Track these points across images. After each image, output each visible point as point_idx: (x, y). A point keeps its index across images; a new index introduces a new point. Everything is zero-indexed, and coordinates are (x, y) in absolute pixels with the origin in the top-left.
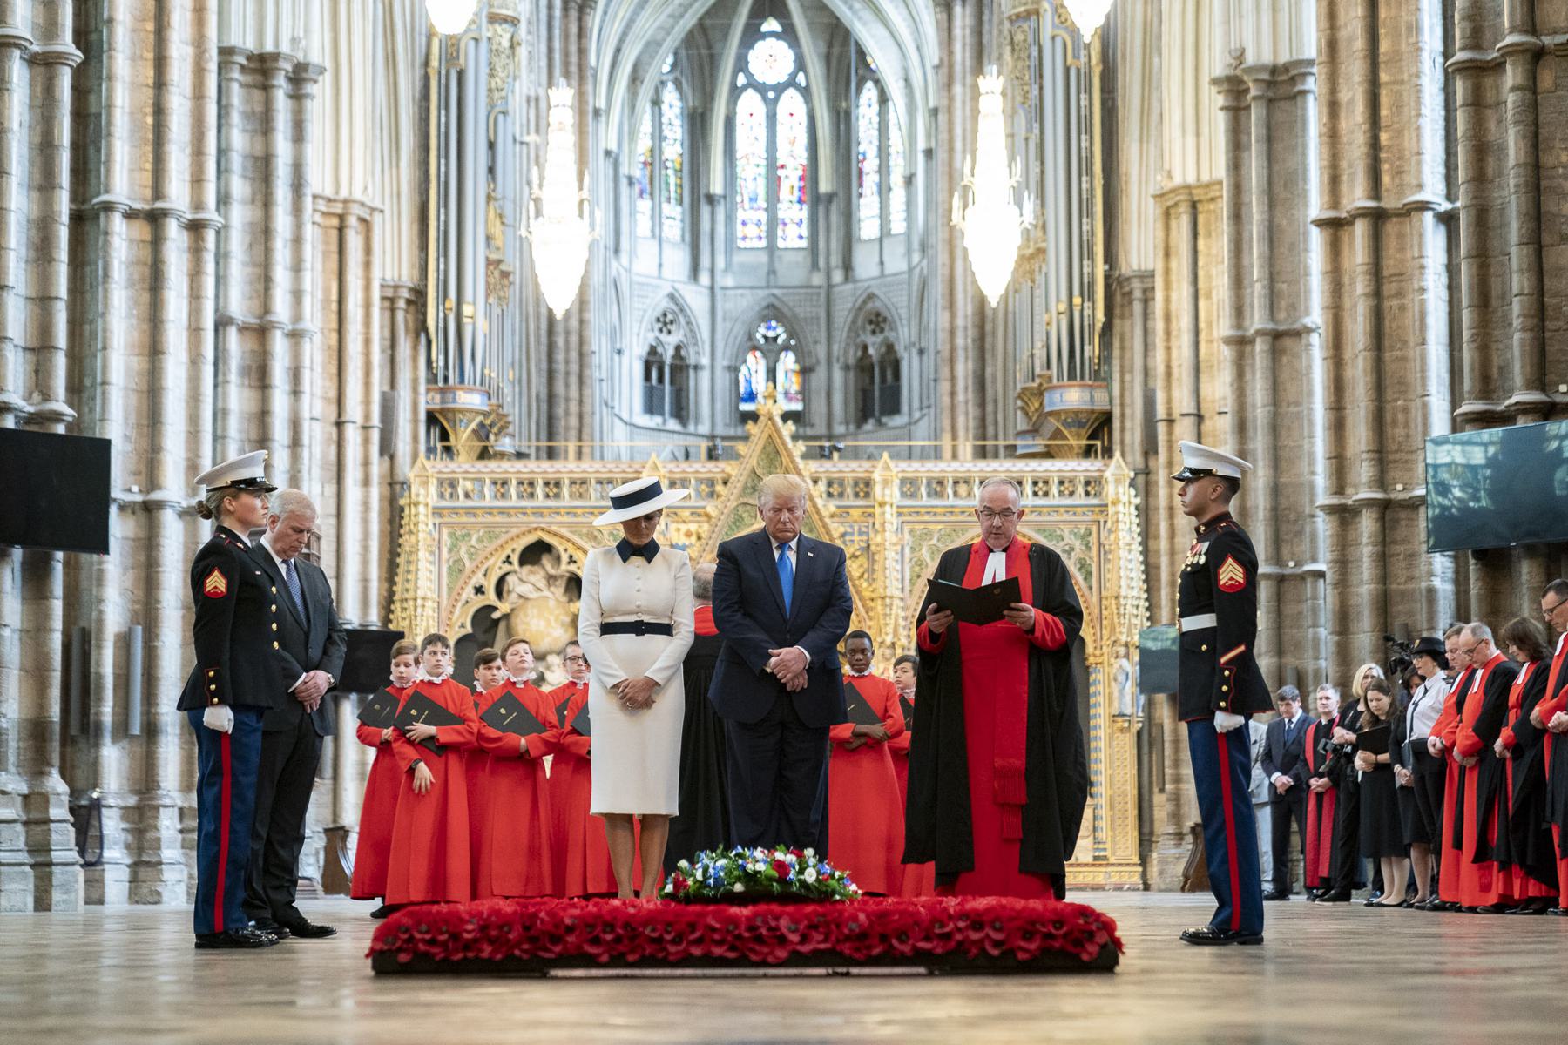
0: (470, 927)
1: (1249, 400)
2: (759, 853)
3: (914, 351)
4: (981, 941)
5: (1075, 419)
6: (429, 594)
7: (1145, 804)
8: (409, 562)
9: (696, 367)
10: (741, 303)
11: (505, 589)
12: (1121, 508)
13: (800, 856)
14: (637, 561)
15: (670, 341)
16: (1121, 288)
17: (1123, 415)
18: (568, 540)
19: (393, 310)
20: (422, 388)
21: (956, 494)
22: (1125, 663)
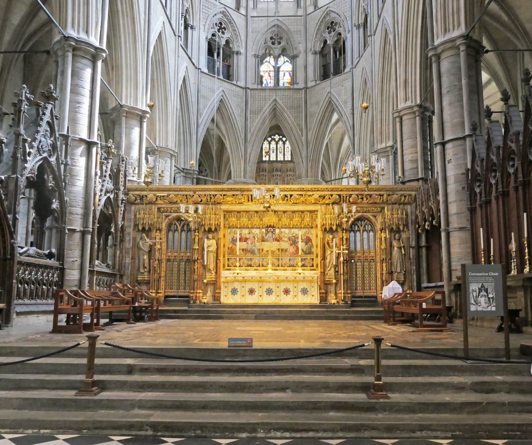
9: (238, 53)
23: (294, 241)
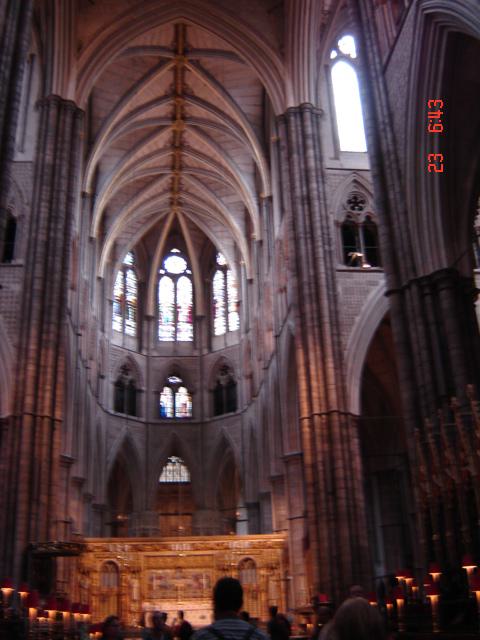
10: (161, 364)
15: (130, 377)
23: (197, 578)
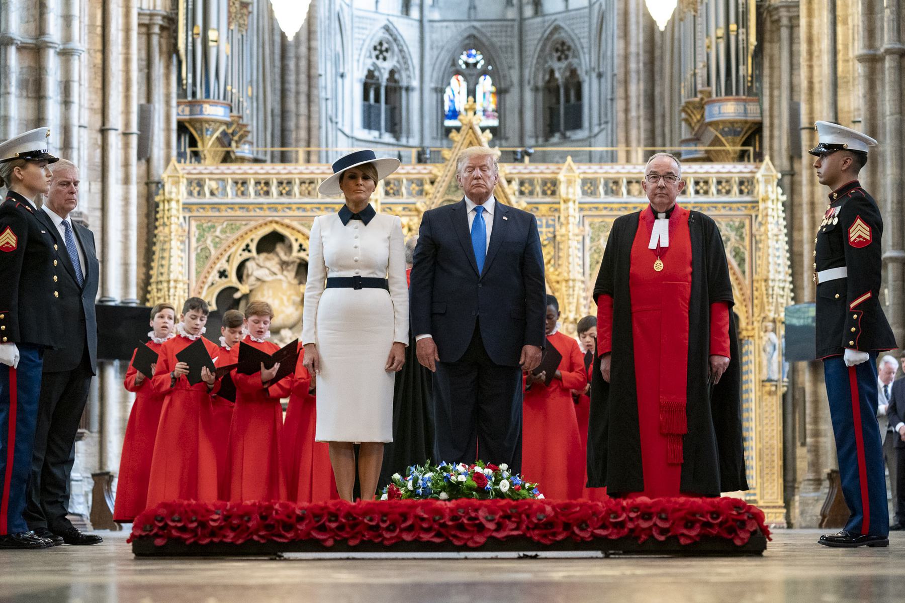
0: (216, 517)
1: (879, 109)
2: (460, 468)
3: (594, 75)
4: (650, 528)
5: (731, 128)
6: (180, 278)
7: (789, 456)
8: (163, 250)
9: (408, 89)
11: (245, 272)
12: (769, 204)
13: (496, 470)
14: (355, 224)
15: (386, 67)
16: (771, 16)
17: (772, 125)
18: (299, 232)
19: (149, 35)
20: (174, 102)
21: (629, 192)
22: (772, 336)
